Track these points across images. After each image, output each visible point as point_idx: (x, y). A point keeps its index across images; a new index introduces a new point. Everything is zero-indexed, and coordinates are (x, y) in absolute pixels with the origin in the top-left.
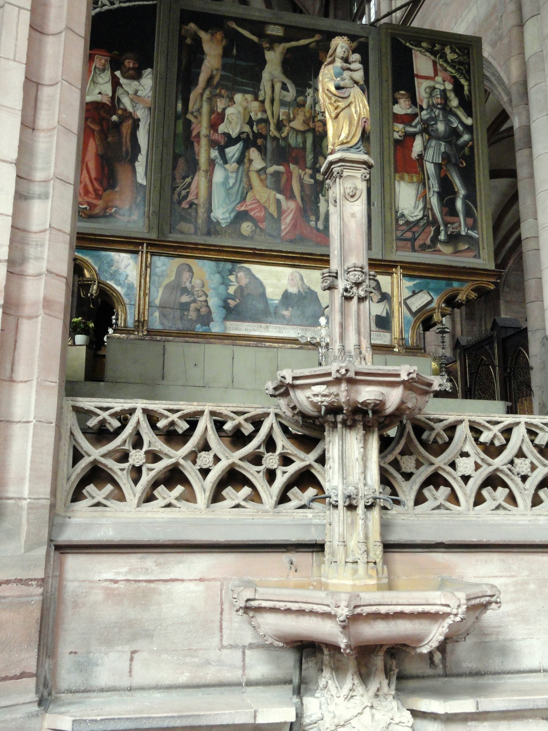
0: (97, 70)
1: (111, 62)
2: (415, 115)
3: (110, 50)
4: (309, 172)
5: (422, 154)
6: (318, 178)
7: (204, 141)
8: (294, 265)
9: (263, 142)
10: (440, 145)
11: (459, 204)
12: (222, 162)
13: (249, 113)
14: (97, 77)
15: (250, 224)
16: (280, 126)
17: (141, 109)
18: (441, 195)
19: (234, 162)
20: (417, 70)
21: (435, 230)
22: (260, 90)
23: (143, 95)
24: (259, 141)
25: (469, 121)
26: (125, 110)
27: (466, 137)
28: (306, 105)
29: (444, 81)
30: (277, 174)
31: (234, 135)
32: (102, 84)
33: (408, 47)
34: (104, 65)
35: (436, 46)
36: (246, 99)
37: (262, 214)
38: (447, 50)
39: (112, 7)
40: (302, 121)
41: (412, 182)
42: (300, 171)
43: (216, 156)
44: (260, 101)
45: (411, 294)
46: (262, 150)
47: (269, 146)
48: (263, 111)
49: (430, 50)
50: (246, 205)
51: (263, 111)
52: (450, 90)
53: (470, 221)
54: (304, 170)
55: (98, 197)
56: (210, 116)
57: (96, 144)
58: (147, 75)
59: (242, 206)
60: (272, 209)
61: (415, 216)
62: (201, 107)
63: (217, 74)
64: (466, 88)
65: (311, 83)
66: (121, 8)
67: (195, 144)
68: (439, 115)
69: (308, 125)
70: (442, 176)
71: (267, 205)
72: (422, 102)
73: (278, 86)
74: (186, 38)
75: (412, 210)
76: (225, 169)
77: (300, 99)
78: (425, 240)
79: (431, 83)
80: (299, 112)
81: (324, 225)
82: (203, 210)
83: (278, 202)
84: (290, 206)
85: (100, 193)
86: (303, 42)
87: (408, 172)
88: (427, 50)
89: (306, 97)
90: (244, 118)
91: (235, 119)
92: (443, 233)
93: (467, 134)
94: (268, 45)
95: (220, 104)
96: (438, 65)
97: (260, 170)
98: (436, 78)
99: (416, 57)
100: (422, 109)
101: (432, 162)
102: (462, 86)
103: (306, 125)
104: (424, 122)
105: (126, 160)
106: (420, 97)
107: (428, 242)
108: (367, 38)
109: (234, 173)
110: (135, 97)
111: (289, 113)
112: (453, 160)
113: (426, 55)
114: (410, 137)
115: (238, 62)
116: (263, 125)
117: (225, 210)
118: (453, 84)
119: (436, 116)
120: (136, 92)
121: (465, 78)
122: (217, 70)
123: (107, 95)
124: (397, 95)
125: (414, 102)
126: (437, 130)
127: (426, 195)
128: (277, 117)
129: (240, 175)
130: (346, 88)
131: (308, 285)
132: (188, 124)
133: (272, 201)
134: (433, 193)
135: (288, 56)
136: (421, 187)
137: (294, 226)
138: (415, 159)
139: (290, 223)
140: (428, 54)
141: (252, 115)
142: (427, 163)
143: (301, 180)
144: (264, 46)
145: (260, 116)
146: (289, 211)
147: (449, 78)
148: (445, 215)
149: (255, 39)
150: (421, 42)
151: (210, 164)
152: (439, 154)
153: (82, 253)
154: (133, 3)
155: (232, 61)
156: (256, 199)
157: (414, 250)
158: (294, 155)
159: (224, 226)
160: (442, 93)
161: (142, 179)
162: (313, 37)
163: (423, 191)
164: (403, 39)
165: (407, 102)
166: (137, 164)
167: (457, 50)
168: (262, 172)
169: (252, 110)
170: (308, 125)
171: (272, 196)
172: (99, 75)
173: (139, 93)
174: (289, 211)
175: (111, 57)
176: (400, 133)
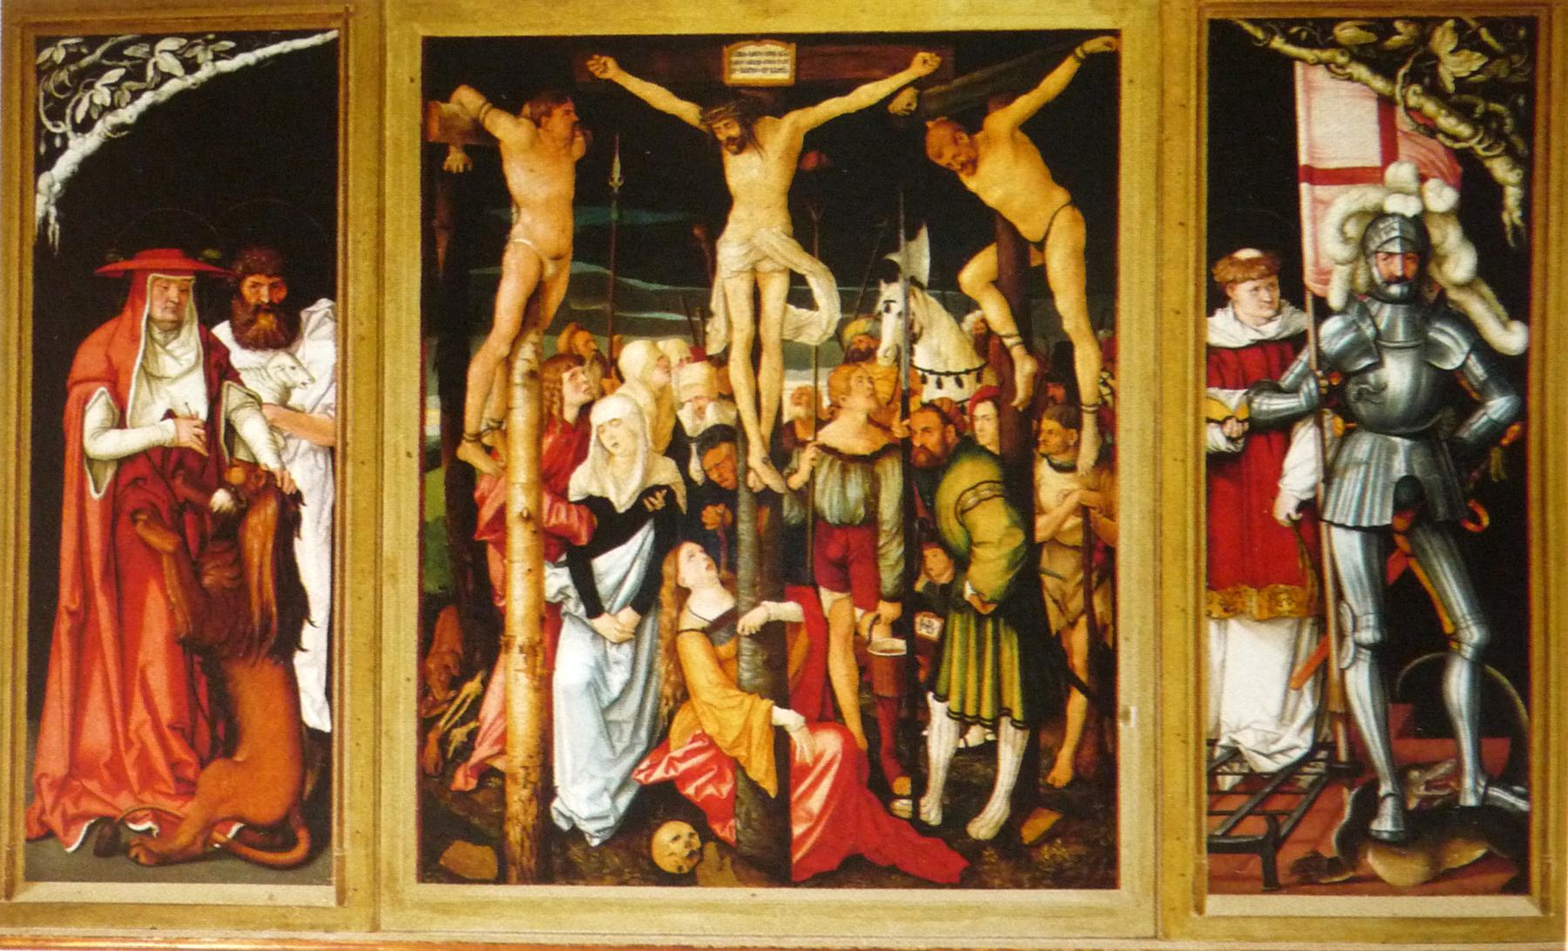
1: (199, 291)
2: (1297, 342)
3: (191, 252)
4: (888, 610)
5: (1315, 498)
6: (922, 631)
7: (520, 539)
9: (722, 516)
10: (1392, 450)
11: (1458, 685)
12: (582, 609)
13: (673, 410)
14: (155, 354)
15: (685, 829)
18: (1385, 658)
19: (624, 606)
21: (1357, 800)
23: (308, 405)
24: (711, 516)
25: (1511, 339)
26: (253, 466)
27: (1498, 406)
28: (880, 353)
29: (1422, 179)
30: (773, 633)
31: (622, 501)
32: (174, 380)
37: (726, 789)
38: (1443, 41)
39: (190, 81)
40: (862, 417)
41: (1272, 617)
42: (859, 612)
43: (561, 591)
44: (710, 359)
46: (721, 548)
47: (745, 529)
48: (722, 397)
50: (672, 759)
52: (1444, 215)
53: (1500, 748)
54: (870, 607)
55: (187, 789)
56: (538, 442)
58: (317, 327)
59: (653, 767)
60: (761, 769)
61: (1281, 752)
62: (508, 409)
63: (557, 275)
64: (1512, 196)
65: (895, 258)
66: (220, 78)
67: (492, 552)
68: (1392, 326)
69: (887, 429)
71: (740, 753)
72: (1326, 282)
73: (776, 290)
74: (447, 153)
75: (1271, 728)
76: (596, 634)
77: (860, 326)
78: (1317, 842)
79: (1367, 196)
82: (525, 793)
83: (781, 737)
84: (820, 748)
85: (190, 773)
86: (867, 95)
87: (1257, 584)
91: (626, 443)
92: (1388, 807)
93: (1503, 395)
95: (573, 389)
100: (1323, 311)
101: (1357, 528)
102: (1498, 190)
104: (1330, 364)
105: (264, 651)
106: (1316, 263)
107: (1330, 849)
110: (285, 415)
112: (1441, 511)
114: (1272, 435)
116: (724, 448)
117: (598, 784)
118: (1455, 186)
119: (1378, 335)
120: (287, 391)
121: (1510, 151)
122: (557, 258)
123: (192, 418)
124: (1224, 271)
125: (1291, 288)
126: (1381, 388)
128: (774, 408)
132: (463, 477)
133: (759, 734)
134: (1357, 653)
135: (811, 162)
136: (1306, 632)
141: (686, 417)
143: (860, 646)
144: (721, 137)
147: (1443, 161)
148: (1403, 734)
149: (688, 111)
151: (542, 621)
152: (1385, 487)
156: (703, 736)
157: (1271, 885)
158: (834, 551)
159: (595, 842)
160: (1411, 232)
161: (319, 714)
162: (906, 65)
163: (1314, 647)
165: (1265, 295)
166: (299, 659)
167: (1484, 34)
168: (722, 634)
169: (684, 397)
170: (887, 429)
171: (758, 722)
172: (163, 347)
173: (296, 399)
176: (1234, 428)
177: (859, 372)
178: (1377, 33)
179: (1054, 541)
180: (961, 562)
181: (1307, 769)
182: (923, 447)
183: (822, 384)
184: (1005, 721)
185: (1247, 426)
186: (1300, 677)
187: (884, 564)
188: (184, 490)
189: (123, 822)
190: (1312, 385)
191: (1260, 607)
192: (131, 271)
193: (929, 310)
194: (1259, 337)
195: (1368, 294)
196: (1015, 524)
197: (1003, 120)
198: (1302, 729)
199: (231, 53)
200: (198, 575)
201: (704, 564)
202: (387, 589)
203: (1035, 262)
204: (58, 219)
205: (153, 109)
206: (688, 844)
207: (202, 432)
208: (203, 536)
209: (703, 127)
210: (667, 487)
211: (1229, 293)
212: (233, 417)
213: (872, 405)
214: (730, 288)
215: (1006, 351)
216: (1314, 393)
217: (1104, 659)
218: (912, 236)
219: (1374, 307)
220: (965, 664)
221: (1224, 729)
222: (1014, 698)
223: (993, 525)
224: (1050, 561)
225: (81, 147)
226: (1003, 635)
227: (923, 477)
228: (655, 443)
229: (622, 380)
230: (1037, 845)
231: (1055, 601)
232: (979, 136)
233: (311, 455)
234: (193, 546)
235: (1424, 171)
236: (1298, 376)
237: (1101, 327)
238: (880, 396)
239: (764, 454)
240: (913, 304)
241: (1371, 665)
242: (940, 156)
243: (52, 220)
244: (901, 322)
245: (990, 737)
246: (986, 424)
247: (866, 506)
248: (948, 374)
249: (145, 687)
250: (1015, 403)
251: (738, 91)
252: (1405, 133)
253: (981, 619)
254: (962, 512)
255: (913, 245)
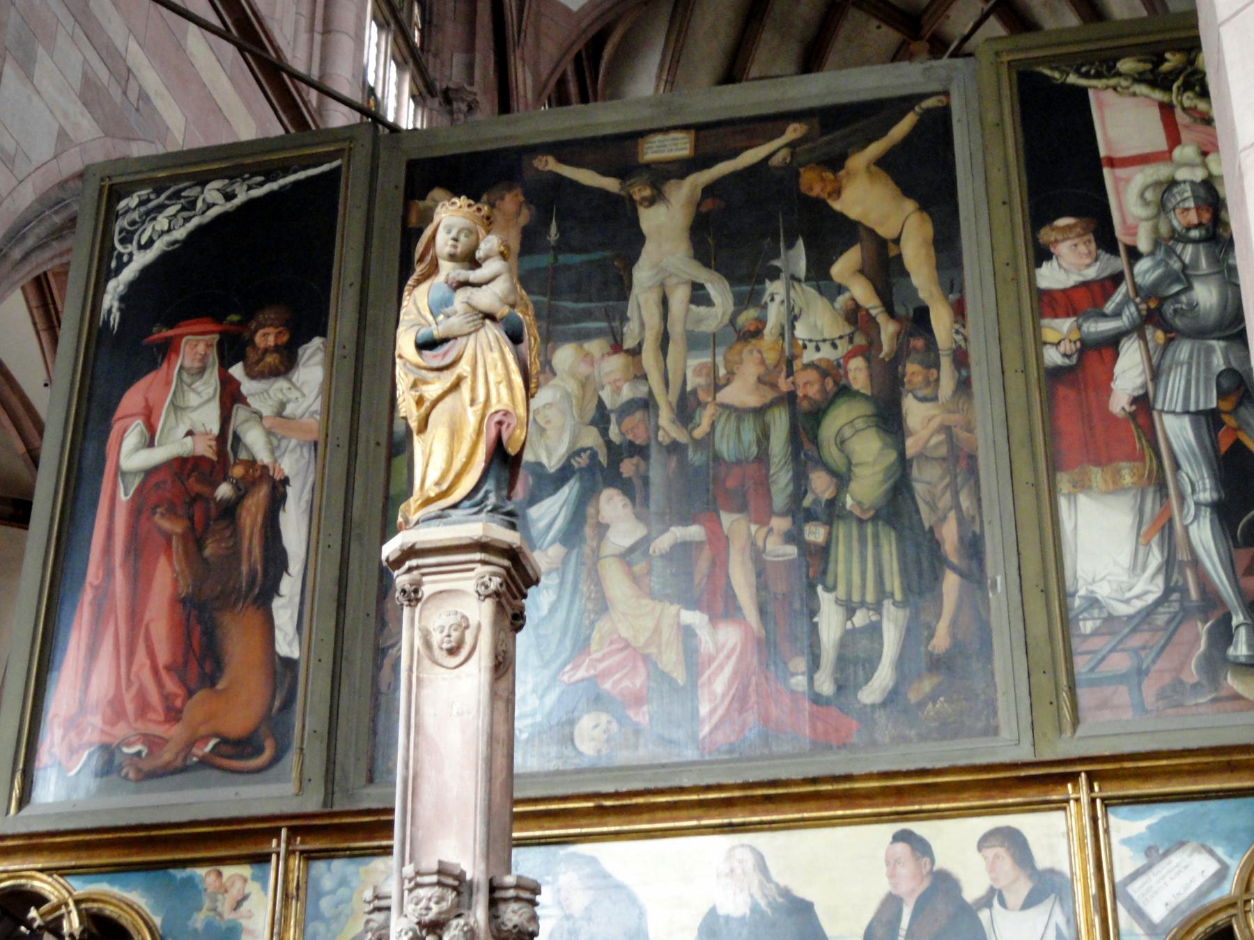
0: (185, 376)
1: (220, 345)
2: (1117, 279)
3: (219, 319)
5: (1146, 395)
8: (731, 825)
9: (637, 466)
10: (1210, 351)
13: (596, 391)
14: (183, 392)
16: (686, 409)
17: (293, 450)
19: (552, 543)
20: (1108, 143)
22: (627, 319)
23: (299, 412)
26: (252, 463)
28: (766, 331)
33: (1073, 87)
34: (204, 358)
35: (1166, 60)
36: (587, 355)
37: (638, 682)
40: (752, 380)
41: (1117, 488)
42: (753, 528)
45: (1141, 861)
46: (633, 490)
48: (636, 377)
49: (1150, 76)
51: (636, 377)
54: (762, 521)
57: (174, 571)
60: (671, 661)
61: (1138, 597)
65: (777, 263)
66: (251, 203)
68: (1195, 259)
69: (774, 386)
70: (1223, 449)
71: (653, 650)
72: (1135, 234)
73: (678, 298)
75: (1125, 578)
77: (749, 315)
79: (1161, 172)
80: (745, 355)
81: (836, 681)
83: (688, 633)
85: (178, 703)
86: (750, 157)
88: (1139, 78)
89: (765, 307)
90: (581, 409)
94: (647, 192)
96: (1178, 111)
97: (632, 549)
98: (1177, 152)
99: (1101, 107)
100: (1134, 254)
103: (767, 388)
105: (249, 600)
106: (1124, 221)
108: (946, 93)
109: (554, 575)
111: (714, 364)
113: (1134, 94)
115: (563, 259)
116: (639, 415)
120: (283, 405)
123: (207, 434)
124: (1046, 235)
125: (1106, 239)
126: (1193, 306)
127: (1171, 520)
128: (680, 381)
129: (570, 578)
130: (455, 338)
131: (782, 883)
133: (667, 633)
135: (708, 205)
137: (740, 701)
138: (1121, 414)
139: (724, 696)
140: (1142, 89)
141: (606, 395)
142: (1169, 420)
144: (637, 197)
145: (627, 392)
146: (722, 656)
149: (611, 184)
150: (1117, 59)
152: (1207, 380)
153: (125, 886)
154: (282, 182)
155: (545, 260)
160: (1202, 192)
161: (290, 644)
162: (782, 133)
164: (1052, 69)
165: (1082, 249)
166: (277, 603)
169: (605, 380)
170: (774, 386)
172: (189, 386)
173: (288, 411)
174: (722, 656)
175: (220, 333)
176: (1067, 347)
177: (749, 347)
178: (1152, 62)
179: (922, 456)
180: (842, 479)
181: (1161, 610)
182: (805, 396)
183: (720, 359)
184: (887, 604)
185: (1078, 344)
186: (1146, 534)
187: (774, 489)
188: (195, 486)
189: (119, 747)
190: (1133, 309)
191: (1106, 481)
192: (171, 338)
193: (807, 296)
194: (1081, 279)
195: (1172, 238)
196: (886, 445)
197: (859, 161)
198: (1153, 577)
199: (261, 184)
200: (200, 544)
201: (620, 505)
202: (354, 547)
203: (893, 252)
204: (120, 309)
205: (200, 229)
206: (606, 731)
207: (213, 443)
208: (208, 518)
209: (623, 193)
210: (591, 448)
211: (1052, 249)
212: (239, 430)
213: (762, 370)
214: (643, 300)
215: (873, 320)
216: (1135, 314)
217: (973, 547)
218: (790, 245)
219: (1179, 248)
220: (849, 561)
221: (1081, 583)
222: (894, 583)
223: (869, 453)
224: (920, 470)
225: (141, 260)
226: (882, 535)
227: (806, 423)
228: (581, 416)
229: (554, 374)
230: (921, 704)
231: (927, 503)
232: (842, 173)
233: (298, 450)
234: (199, 528)
235: (1205, 149)
236: (1118, 304)
237: (951, 291)
238: (768, 362)
239: (672, 416)
240: (792, 293)
241: (1212, 521)
242: (811, 189)
243: (114, 310)
244: (783, 309)
245: (874, 618)
246: (858, 374)
247: (759, 443)
248: (824, 340)
249: (148, 639)
250: (882, 356)
251: (648, 166)
252: (1186, 127)
253: (861, 522)
254: (842, 443)
255: (791, 252)
